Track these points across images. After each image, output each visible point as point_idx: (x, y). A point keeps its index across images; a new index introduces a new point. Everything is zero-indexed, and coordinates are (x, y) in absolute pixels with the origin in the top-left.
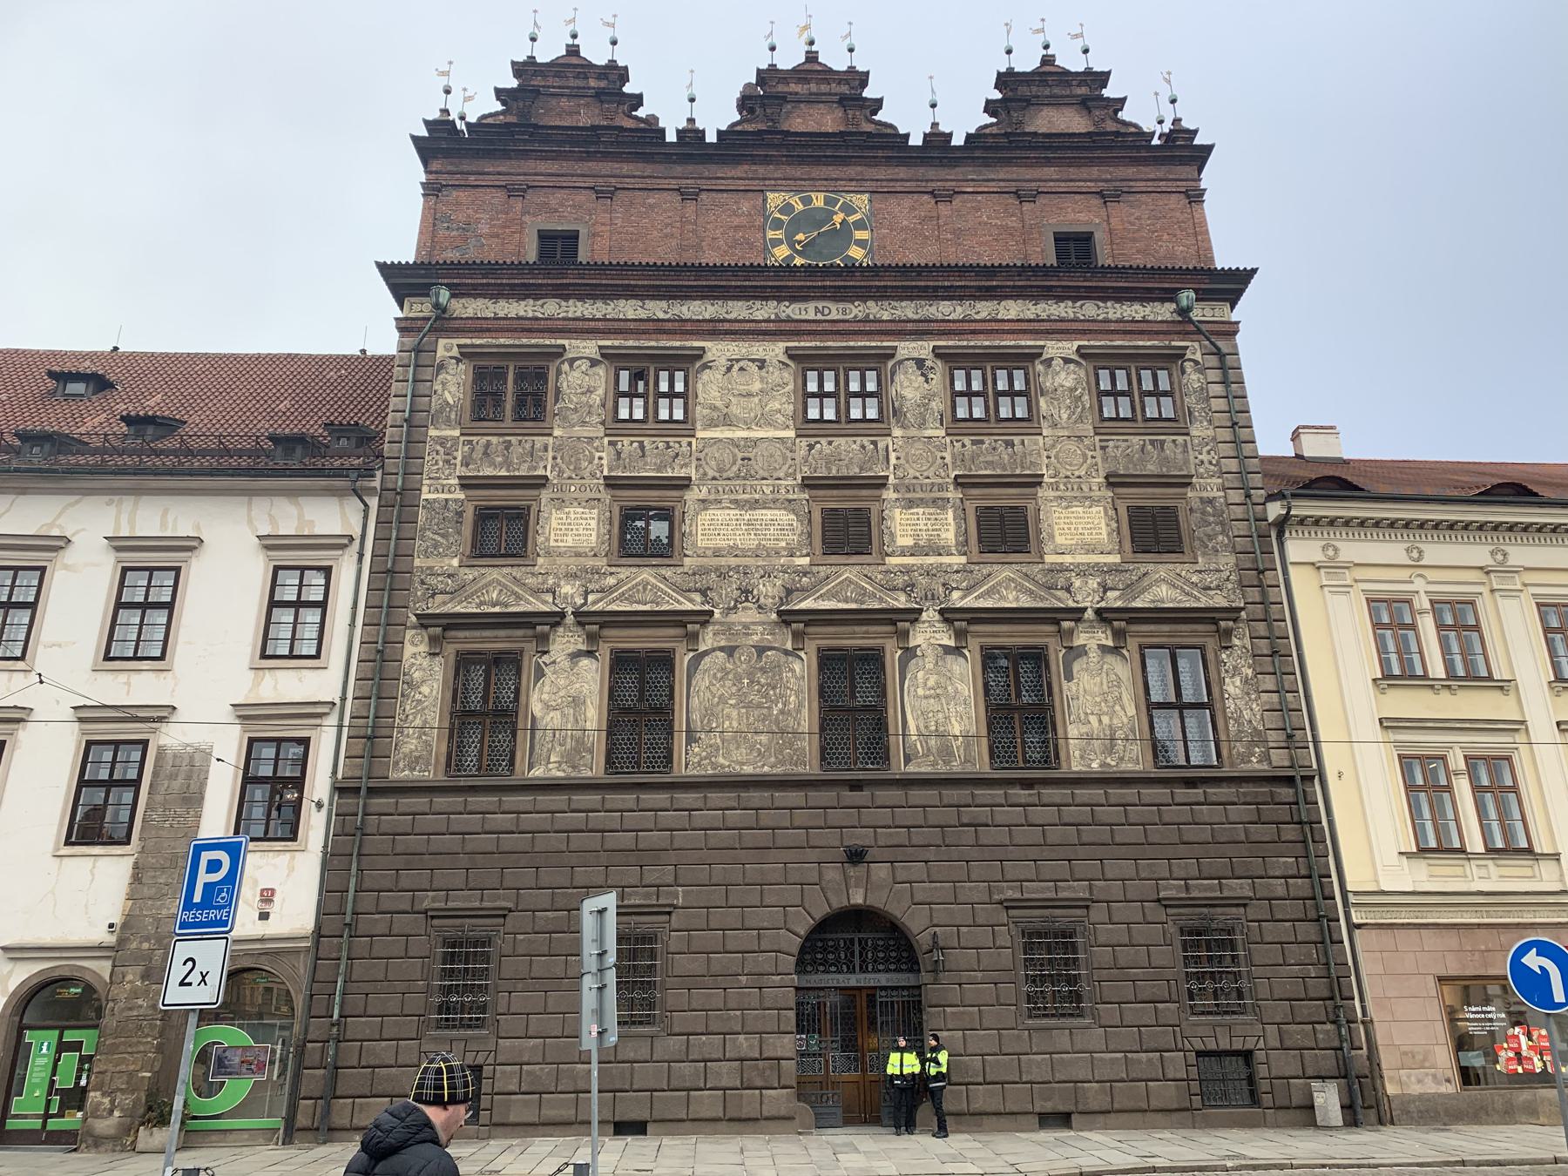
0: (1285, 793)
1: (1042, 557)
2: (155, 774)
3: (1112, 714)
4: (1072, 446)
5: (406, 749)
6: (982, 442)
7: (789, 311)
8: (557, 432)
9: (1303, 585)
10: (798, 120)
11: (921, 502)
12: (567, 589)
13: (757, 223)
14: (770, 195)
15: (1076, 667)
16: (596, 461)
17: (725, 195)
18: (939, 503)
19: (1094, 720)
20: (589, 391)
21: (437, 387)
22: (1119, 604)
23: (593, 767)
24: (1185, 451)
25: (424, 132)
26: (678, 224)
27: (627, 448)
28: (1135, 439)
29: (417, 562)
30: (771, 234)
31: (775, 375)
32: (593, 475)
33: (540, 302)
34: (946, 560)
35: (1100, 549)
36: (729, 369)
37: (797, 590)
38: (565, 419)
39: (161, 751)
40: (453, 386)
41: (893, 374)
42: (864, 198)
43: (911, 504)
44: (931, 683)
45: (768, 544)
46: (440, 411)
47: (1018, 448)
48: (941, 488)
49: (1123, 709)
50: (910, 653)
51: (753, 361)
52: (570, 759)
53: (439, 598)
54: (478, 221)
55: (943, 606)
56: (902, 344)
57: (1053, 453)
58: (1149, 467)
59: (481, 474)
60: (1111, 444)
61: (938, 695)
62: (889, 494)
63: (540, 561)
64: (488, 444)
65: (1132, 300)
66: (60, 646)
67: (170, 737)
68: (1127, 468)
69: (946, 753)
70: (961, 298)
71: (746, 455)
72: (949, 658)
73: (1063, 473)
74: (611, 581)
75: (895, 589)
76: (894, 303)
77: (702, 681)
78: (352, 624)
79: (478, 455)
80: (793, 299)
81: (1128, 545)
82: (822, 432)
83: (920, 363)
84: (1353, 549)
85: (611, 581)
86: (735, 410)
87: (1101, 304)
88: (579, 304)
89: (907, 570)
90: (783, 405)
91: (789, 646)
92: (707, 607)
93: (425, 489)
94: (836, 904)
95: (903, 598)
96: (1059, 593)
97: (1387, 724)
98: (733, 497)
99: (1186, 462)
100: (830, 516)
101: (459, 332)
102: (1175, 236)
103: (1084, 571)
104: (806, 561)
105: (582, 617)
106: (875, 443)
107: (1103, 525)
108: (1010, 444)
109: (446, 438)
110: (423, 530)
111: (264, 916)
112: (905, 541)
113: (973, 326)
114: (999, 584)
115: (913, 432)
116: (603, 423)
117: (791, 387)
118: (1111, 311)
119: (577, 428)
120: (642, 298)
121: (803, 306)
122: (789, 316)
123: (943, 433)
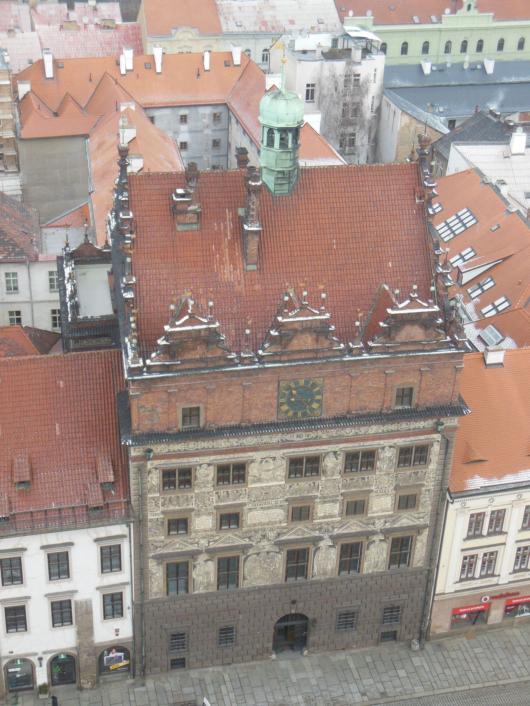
1: (367, 515)
2: (76, 608)
3: (379, 557)
4: (386, 478)
5: (154, 591)
6: (354, 479)
7: (286, 437)
8: (196, 491)
10: (296, 342)
11: (329, 502)
12: (202, 542)
13: (275, 395)
15: (370, 547)
16: (211, 500)
18: (335, 501)
19: (373, 560)
20: (207, 475)
21: (149, 480)
22: (389, 526)
23: (213, 589)
24: (425, 474)
26: (242, 400)
27: (222, 494)
28: (408, 472)
29: (150, 539)
30: (281, 400)
31: (279, 462)
32: (210, 505)
33: (187, 444)
34: (334, 519)
36: (261, 462)
39: (76, 603)
40: (155, 479)
41: (324, 457)
42: (321, 379)
43: (325, 502)
44: (323, 556)
45: (273, 520)
48: (336, 496)
51: (271, 458)
53: (158, 549)
54: (156, 407)
62: (318, 500)
63: (192, 534)
64: (171, 498)
66: (33, 578)
67: (77, 598)
68: (403, 483)
69: (325, 573)
73: (380, 486)
74: (217, 538)
75: (315, 530)
76: (329, 431)
77: (248, 564)
79: (167, 502)
83: (335, 453)
86: (263, 476)
88: (202, 443)
89: (320, 524)
91: (278, 551)
92: (250, 542)
93: (149, 515)
94: (286, 614)
95: (317, 532)
96: (370, 526)
98: (261, 506)
99: (424, 477)
103: (379, 518)
105: (209, 551)
106: (314, 483)
107: (390, 503)
109: (155, 497)
110: (150, 528)
114: (351, 525)
115: (329, 478)
116: (213, 486)
117: (285, 466)
118: (412, 425)
119: (203, 489)
121: (292, 435)
122: (286, 440)
123: (340, 477)
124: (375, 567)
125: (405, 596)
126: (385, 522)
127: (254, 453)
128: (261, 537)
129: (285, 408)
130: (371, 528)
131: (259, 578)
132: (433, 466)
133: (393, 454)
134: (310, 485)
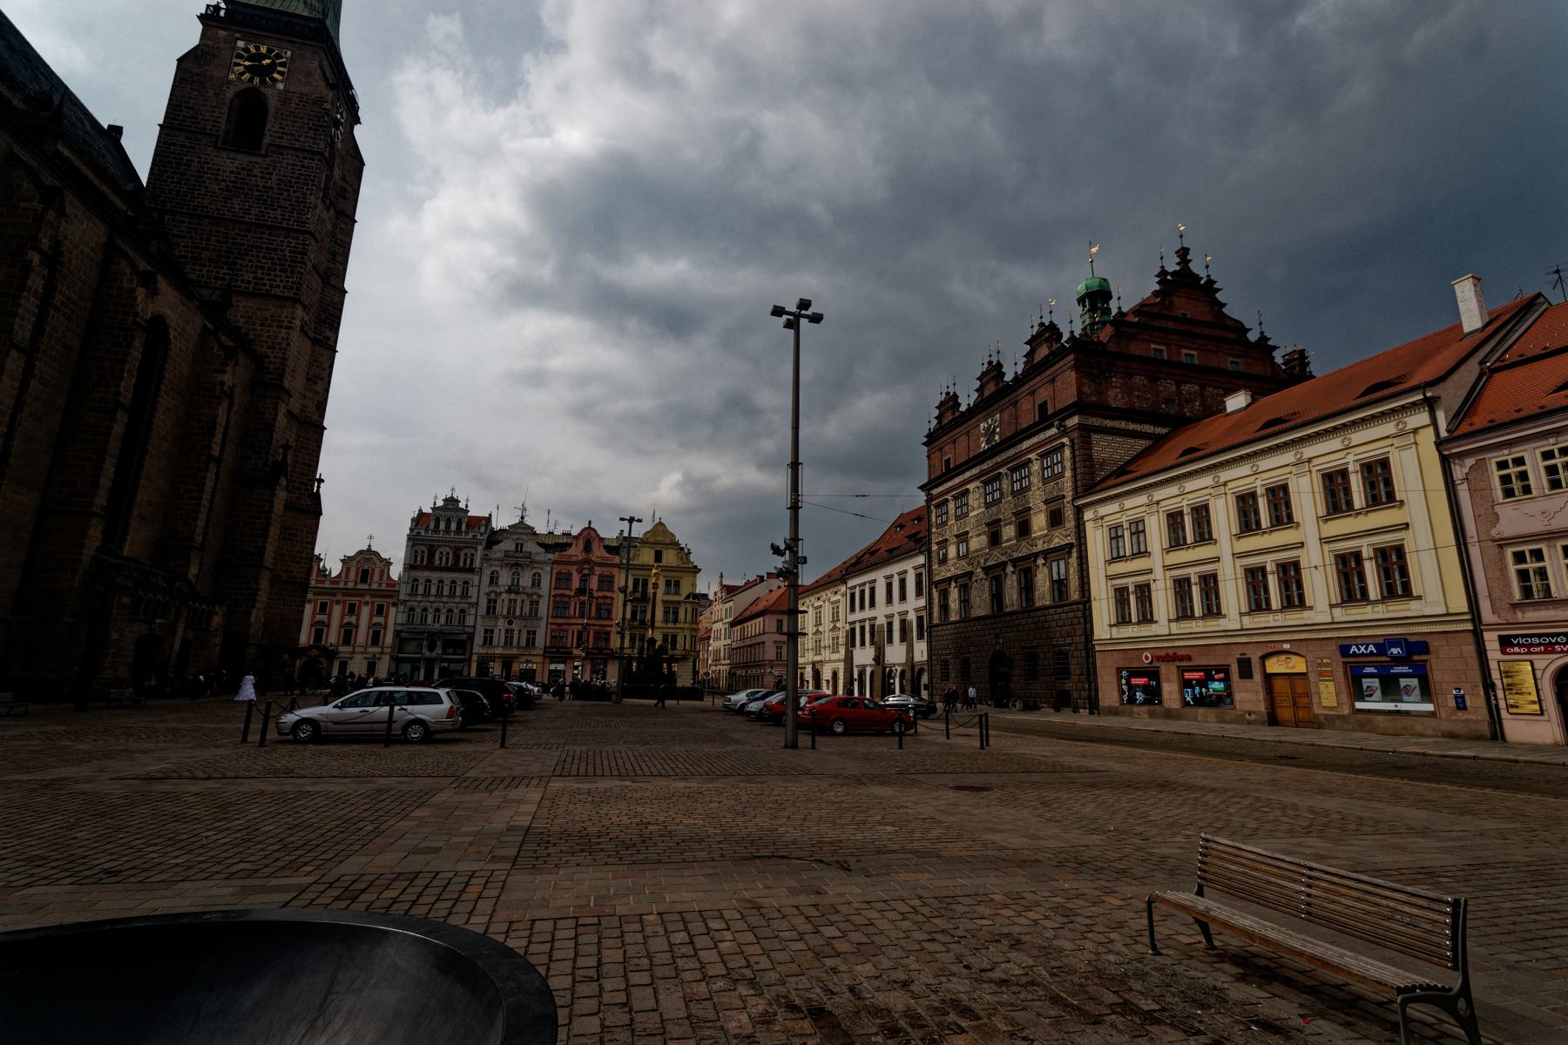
0: (1081, 607)
9: (1089, 527)
18: (1010, 523)
25: (926, 440)
43: (1006, 525)
50: (1006, 574)
69: (1013, 605)
84: (1103, 510)
90: (982, 501)
97: (1110, 578)
100: (992, 533)
125: (1069, 640)
130: (1035, 550)
131: (979, 606)
132: (1068, 474)
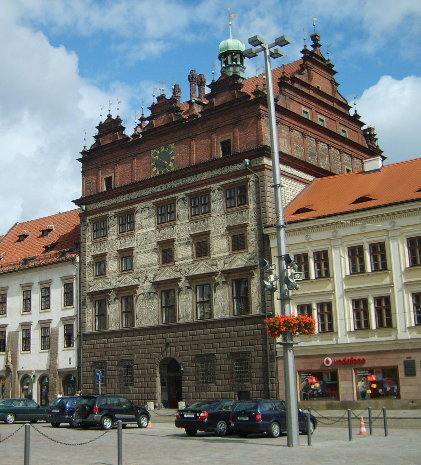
1: (210, 256)
3: (224, 301)
4: (219, 219)
6: (197, 222)
8: (109, 239)
14: (152, 151)
15: (217, 289)
17: (142, 154)
19: (220, 303)
20: (114, 225)
22: (227, 268)
24: (248, 214)
25: (81, 156)
29: (87, 279)
30: (152, 164)
35: (225, 251)
36: (142, 211)
37: (157, 275)
38: (110, 235)
43: (181, 245)
44: (184, 298)
46: (88, 238)
47: (206, 222)
49: (227, 299)
51: (147, 208)
52: (115, 325)
53: (91, 288)
55: (187, 275)
56: (180, 193)
57: (214, 222)
58: (239, 221)
59: (96, 254)
60: (229, 215)
61: (186, 301)
62: (176, 243)
63: (107, 275)
65: (237, 163)
69: (187, 317)
70: (193, 175)
71: (146, 237)
72: (189, 290)
76: (178, 181)
77: (139, 302)
78: (77, 297)
79: (95, 248)
80: (155, 186)
81: (231, 249)
82: (161, 227)
85: (120, 278)
87: (229, 167)
89: (180, 265)
93: (87, 259)
95: (179, 273)
96: (215, 267)
99: (248, 217)
101: (89, 215)
102: (253, 133)
103: (219, 259)
104: (157, 266)
107: (226, 243)
108: (204, 221)
111: (70, 363)
112: (180, 257)
113: (196, 184)
114: (200, 266)
115: (182, 222)
118: (231, 168)
120: (123, 195)
121: (156, 187)
123: (188, 221)
124: (223, 311)
126: (225, 263)
127: (137, 205)
128: (145, 278)
129: (154, 169)
130: (214, 269)
131: (146, 318)
132: (252, 205)
133: (221, 196)
134: (171, 229)
